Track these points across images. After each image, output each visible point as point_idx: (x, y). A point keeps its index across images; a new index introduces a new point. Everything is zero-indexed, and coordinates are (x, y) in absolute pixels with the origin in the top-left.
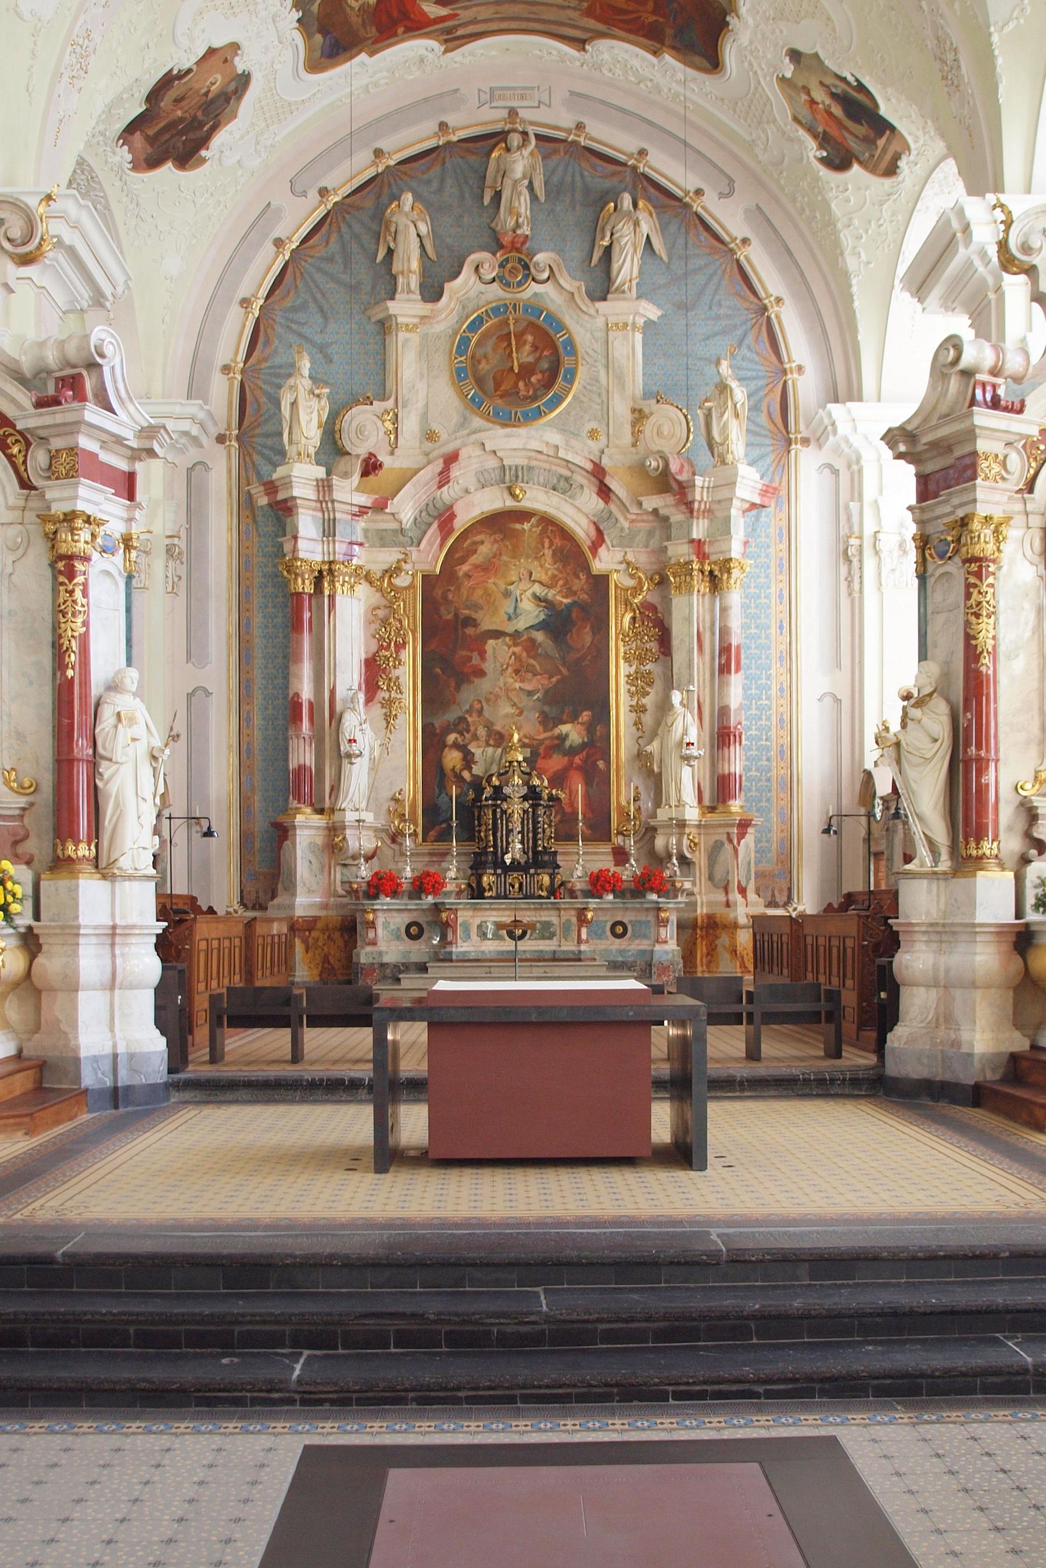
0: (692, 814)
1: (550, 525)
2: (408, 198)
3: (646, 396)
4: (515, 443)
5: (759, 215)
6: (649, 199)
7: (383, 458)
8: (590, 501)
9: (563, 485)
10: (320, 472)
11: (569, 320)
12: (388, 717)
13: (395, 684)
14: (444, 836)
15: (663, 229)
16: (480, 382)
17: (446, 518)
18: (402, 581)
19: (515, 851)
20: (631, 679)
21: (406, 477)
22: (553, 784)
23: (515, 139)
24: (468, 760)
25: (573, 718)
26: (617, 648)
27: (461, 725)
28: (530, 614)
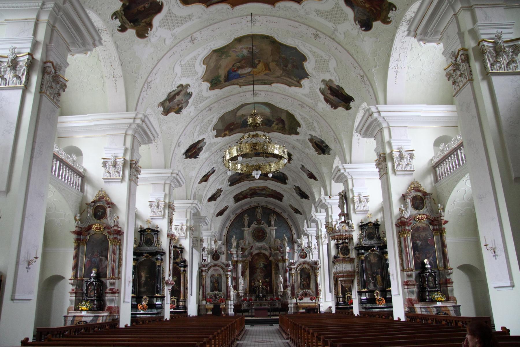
0: (282, 290)
1: (264, 254)
2: (246, 215)
3: (276, 238)
4: (260, 245)
5: (289, 215)
6: (275, 214)
7: (244, 247)
8: (269, 251)
9: (266, 249)
10: (236, 249)
11: (266, 229)
12: (245, 279)
13: (245, 275)
14: (252, 294)
15: (277, 217)
16: (255, 237)
17: (251, 254)
18: (246, 262)
19: (261, 295)
20: (275, 273)
21: (246, 249)
22: (265, 287)
23: (259, 208)
24: (255, 284)
25: (267, 278)
26: (273, 270)
27: (254, 279)
28: (262, 265)
